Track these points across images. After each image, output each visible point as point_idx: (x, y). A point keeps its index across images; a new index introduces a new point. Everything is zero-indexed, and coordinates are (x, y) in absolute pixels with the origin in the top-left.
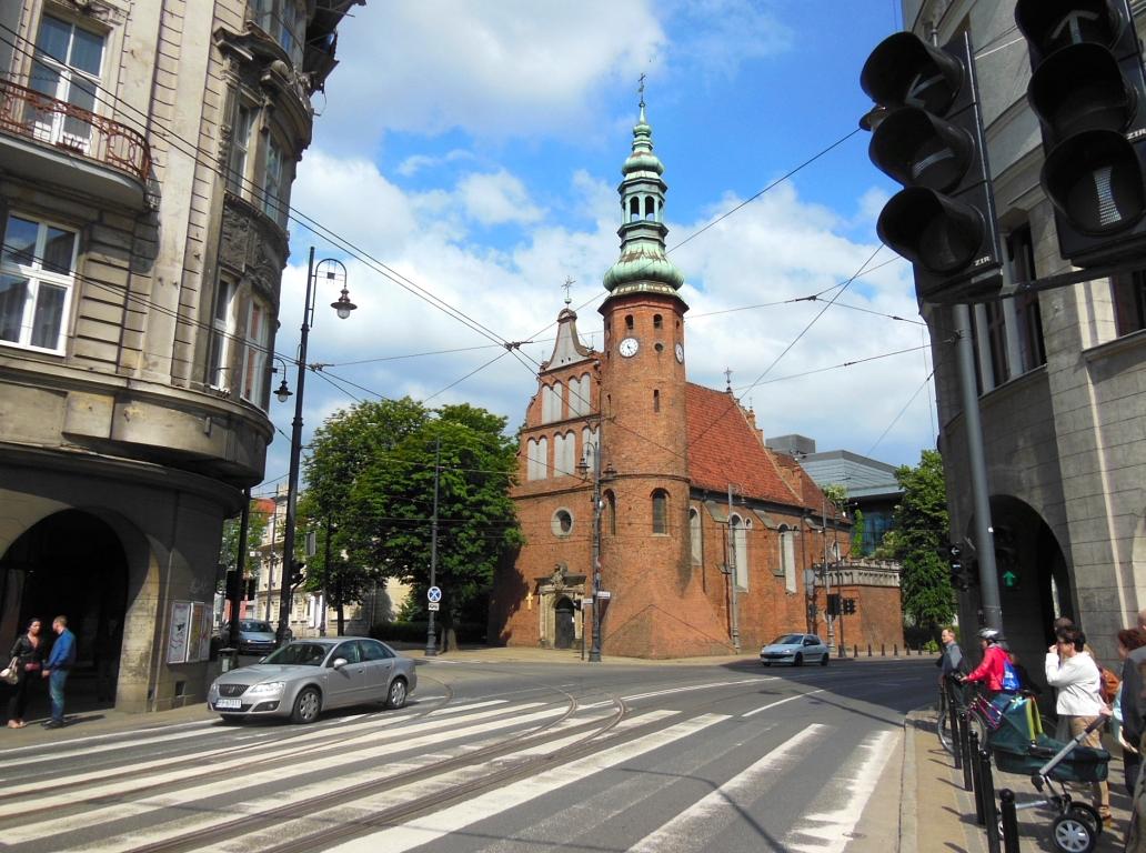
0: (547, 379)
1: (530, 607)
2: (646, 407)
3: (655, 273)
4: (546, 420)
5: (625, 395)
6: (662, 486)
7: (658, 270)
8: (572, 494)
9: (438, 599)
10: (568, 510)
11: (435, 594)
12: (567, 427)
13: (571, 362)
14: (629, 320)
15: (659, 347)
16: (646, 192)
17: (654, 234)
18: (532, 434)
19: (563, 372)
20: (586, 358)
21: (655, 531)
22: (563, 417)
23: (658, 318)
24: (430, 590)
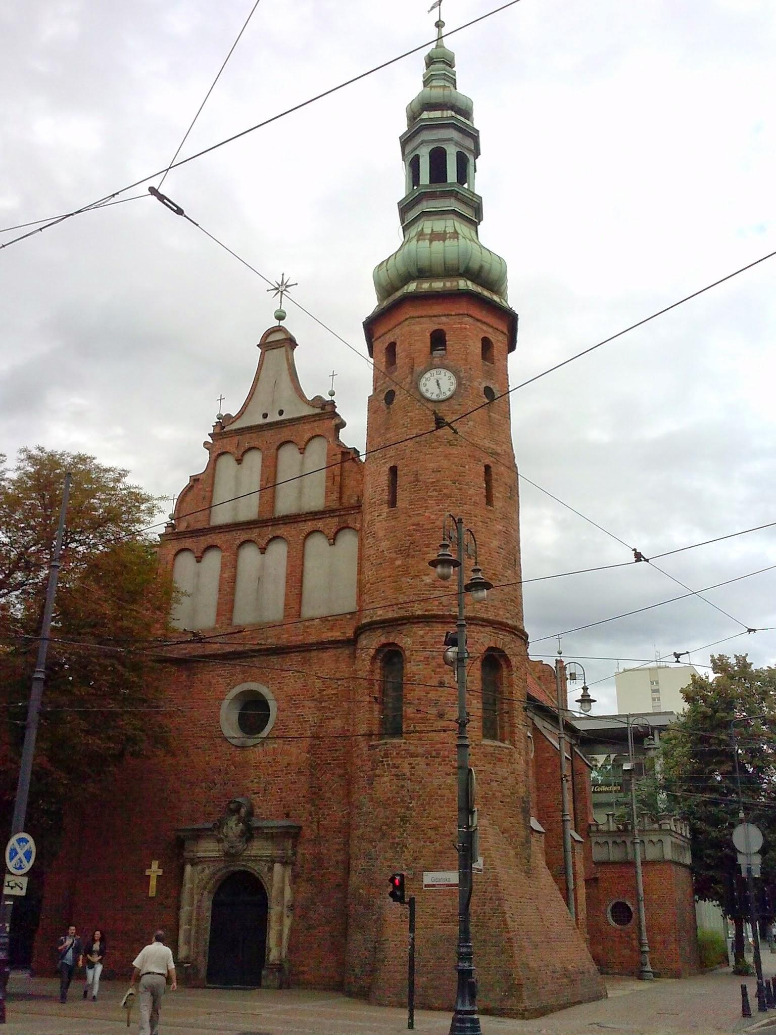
0: (229, 444)
1: (152, 892)
2: (472, 492)
3: (481, 267)
4: (222, 516)
5: (431, 465)
6: (500, 646)
7: (487, 266)
8: (274, 659)
9: (28, 866)
10: (264, 690)
11: (21, 854)
12: (270, 532)
13: (283, 417)
14: (438, 340)
15: (488, 392)
16: (457, 144)
17: (468, 212)
18: (187, 543)
19: (268, 434)
20: (318, 411)
21: (485, 736)
22: (260, 512)
23: (486, 344)
24: (13, 841)
